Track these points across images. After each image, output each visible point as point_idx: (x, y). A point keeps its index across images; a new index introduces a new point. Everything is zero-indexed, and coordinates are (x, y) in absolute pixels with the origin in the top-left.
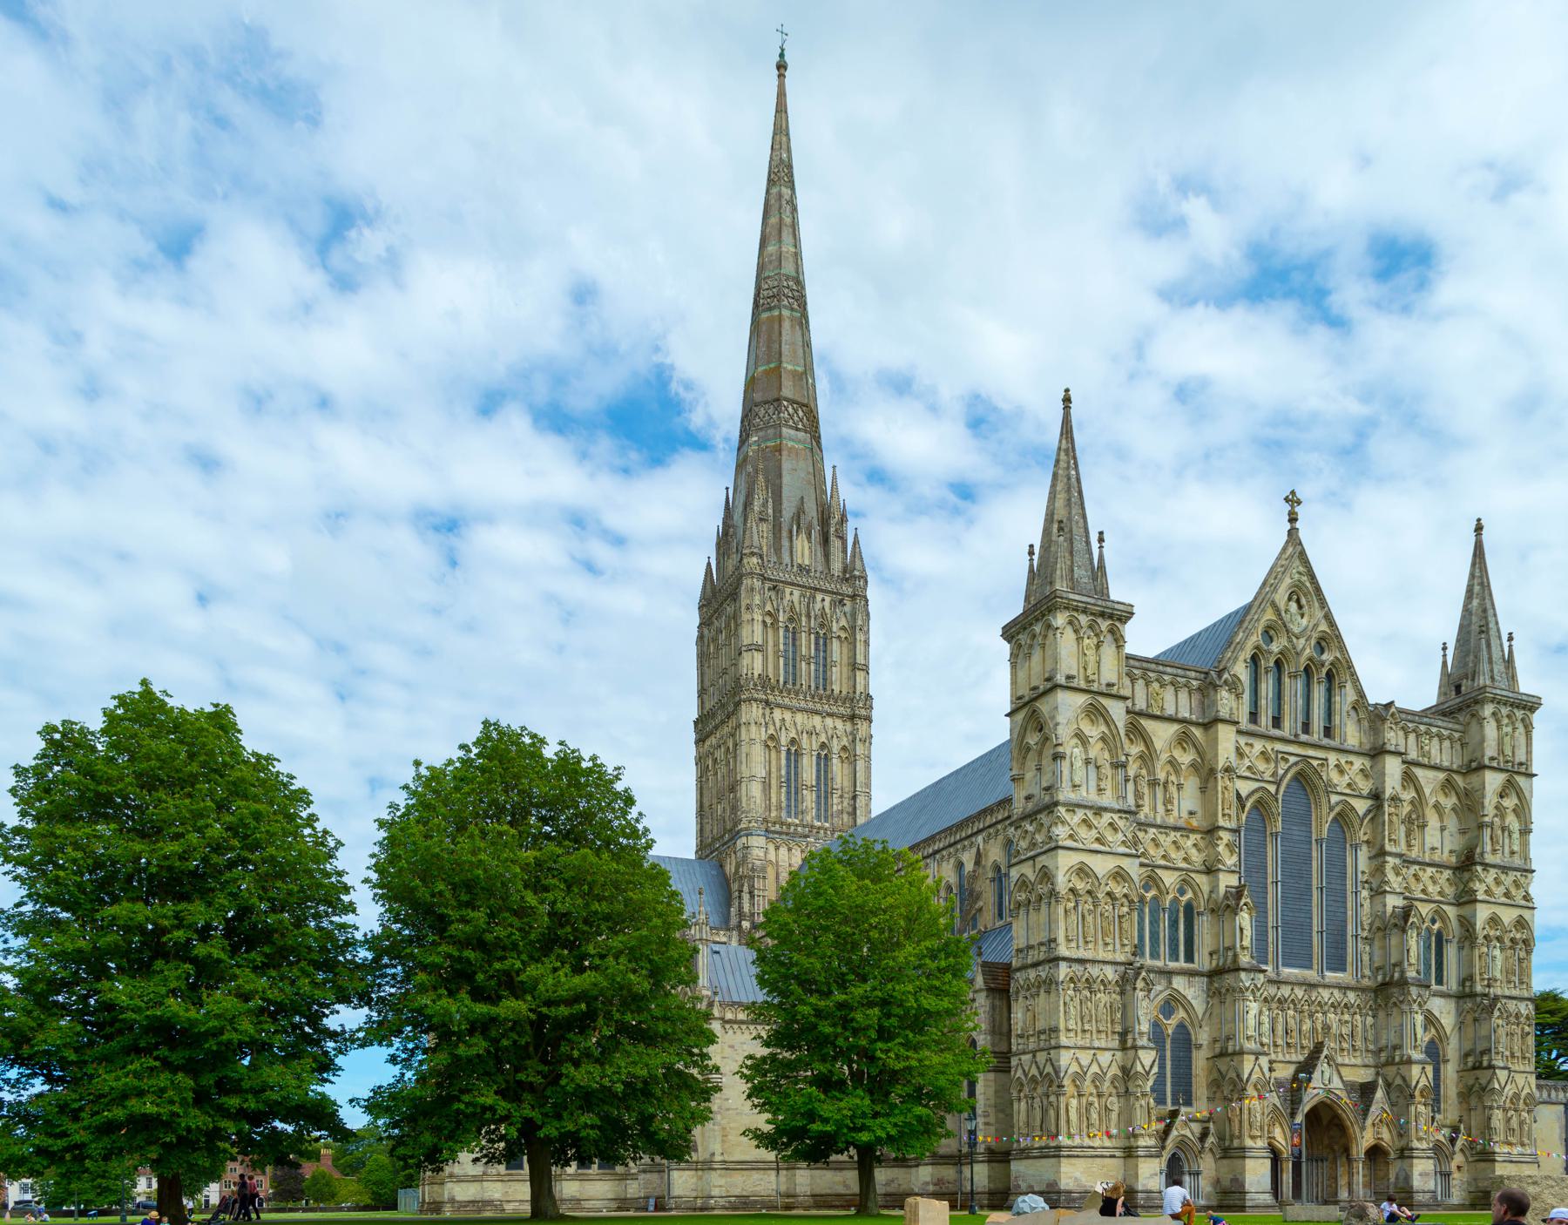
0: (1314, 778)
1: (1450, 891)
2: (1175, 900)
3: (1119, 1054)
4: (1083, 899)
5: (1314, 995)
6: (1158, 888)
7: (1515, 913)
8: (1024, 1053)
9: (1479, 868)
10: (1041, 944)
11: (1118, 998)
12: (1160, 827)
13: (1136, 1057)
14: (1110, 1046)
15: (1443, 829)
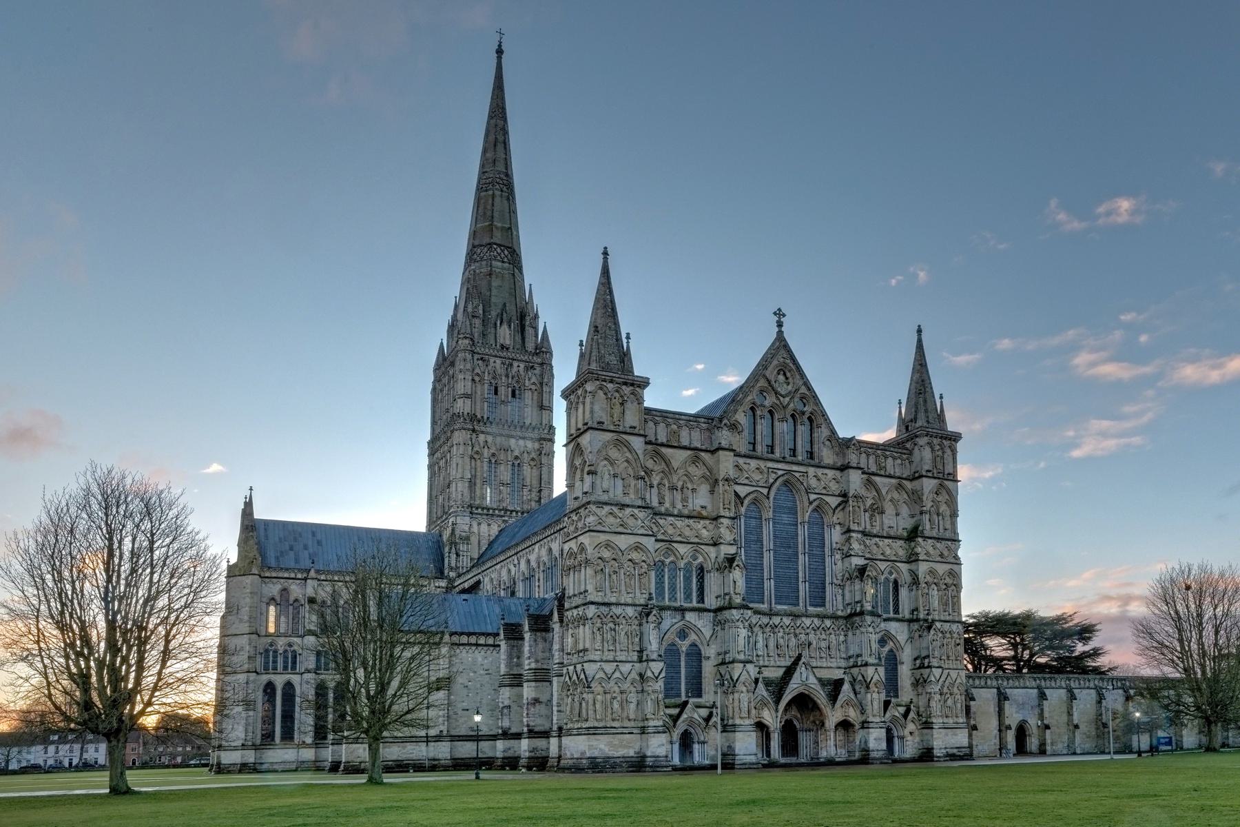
0: (798, 484)
1: (901, 553)
2: (689, 563)
3: (637, 665)
4: (610, 564)
5: (798, 623)
6: (675, 555)
7: (948, 567)
8: (570, 665)
9: (920, 540)
10: (581, 593)
11: (637, 628)
12: (677, 516)
13: (648, 667)
14: (630, 659)
15: (897, 515)
